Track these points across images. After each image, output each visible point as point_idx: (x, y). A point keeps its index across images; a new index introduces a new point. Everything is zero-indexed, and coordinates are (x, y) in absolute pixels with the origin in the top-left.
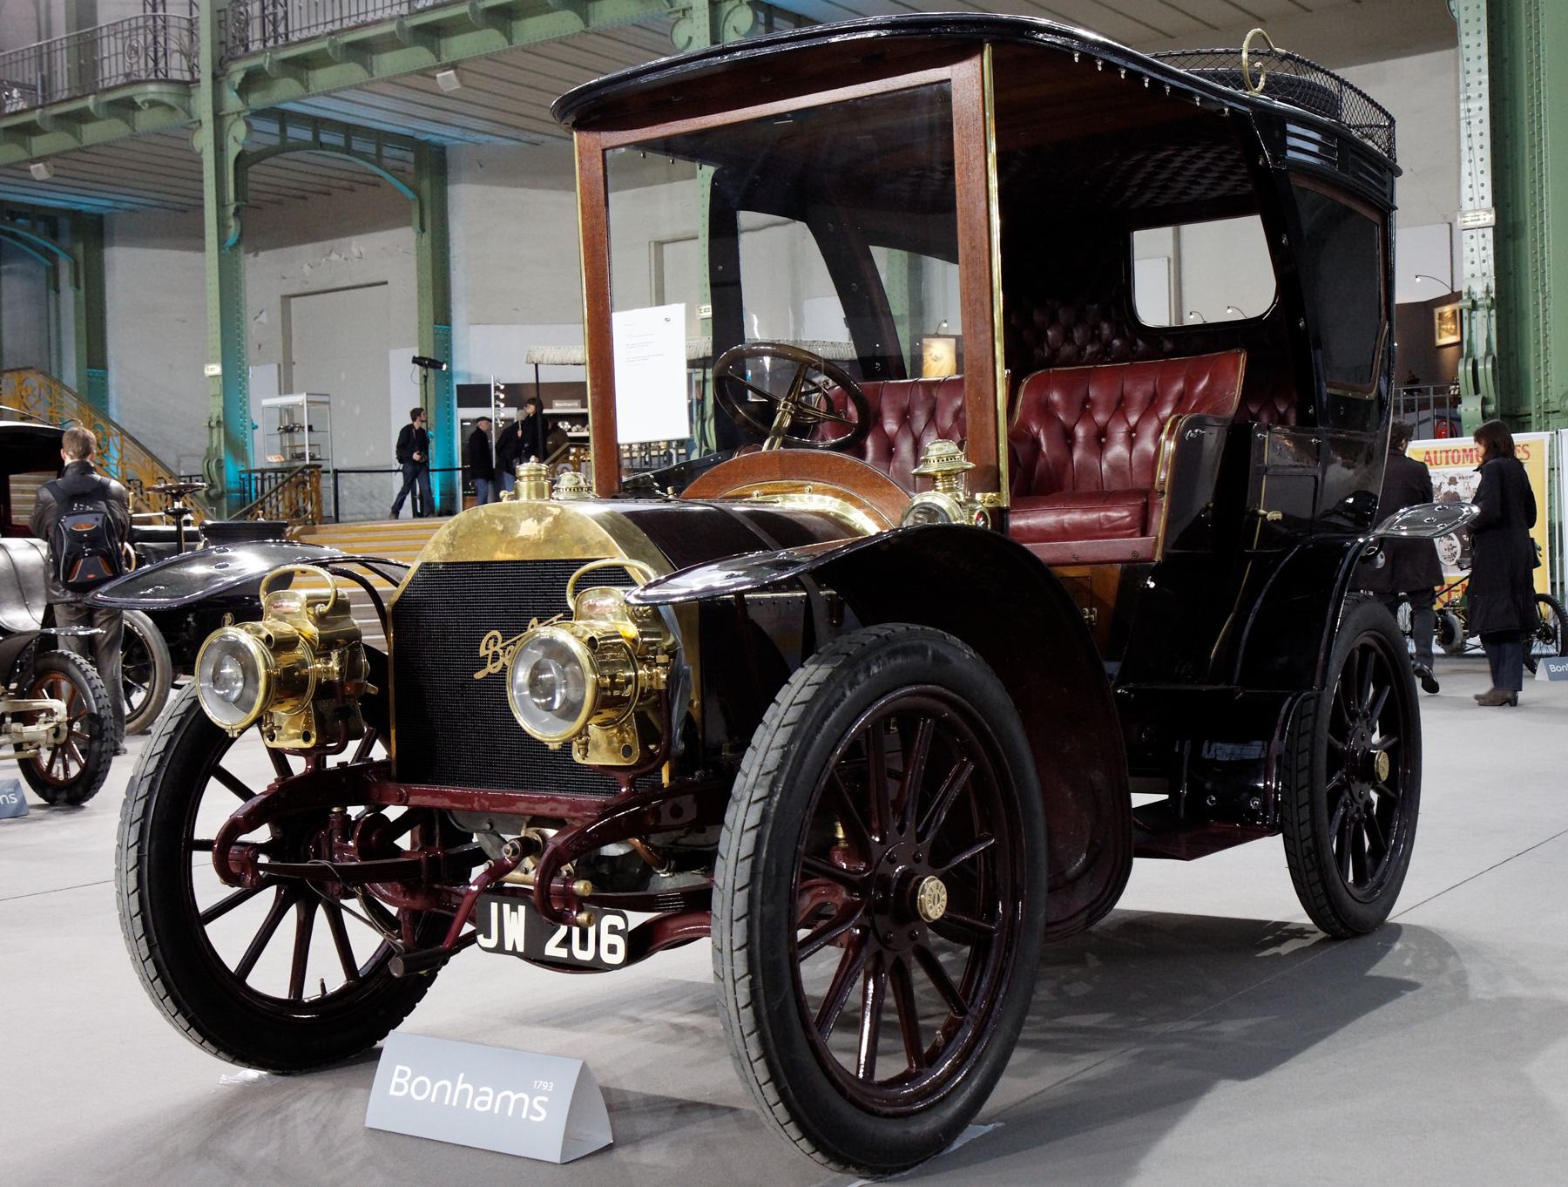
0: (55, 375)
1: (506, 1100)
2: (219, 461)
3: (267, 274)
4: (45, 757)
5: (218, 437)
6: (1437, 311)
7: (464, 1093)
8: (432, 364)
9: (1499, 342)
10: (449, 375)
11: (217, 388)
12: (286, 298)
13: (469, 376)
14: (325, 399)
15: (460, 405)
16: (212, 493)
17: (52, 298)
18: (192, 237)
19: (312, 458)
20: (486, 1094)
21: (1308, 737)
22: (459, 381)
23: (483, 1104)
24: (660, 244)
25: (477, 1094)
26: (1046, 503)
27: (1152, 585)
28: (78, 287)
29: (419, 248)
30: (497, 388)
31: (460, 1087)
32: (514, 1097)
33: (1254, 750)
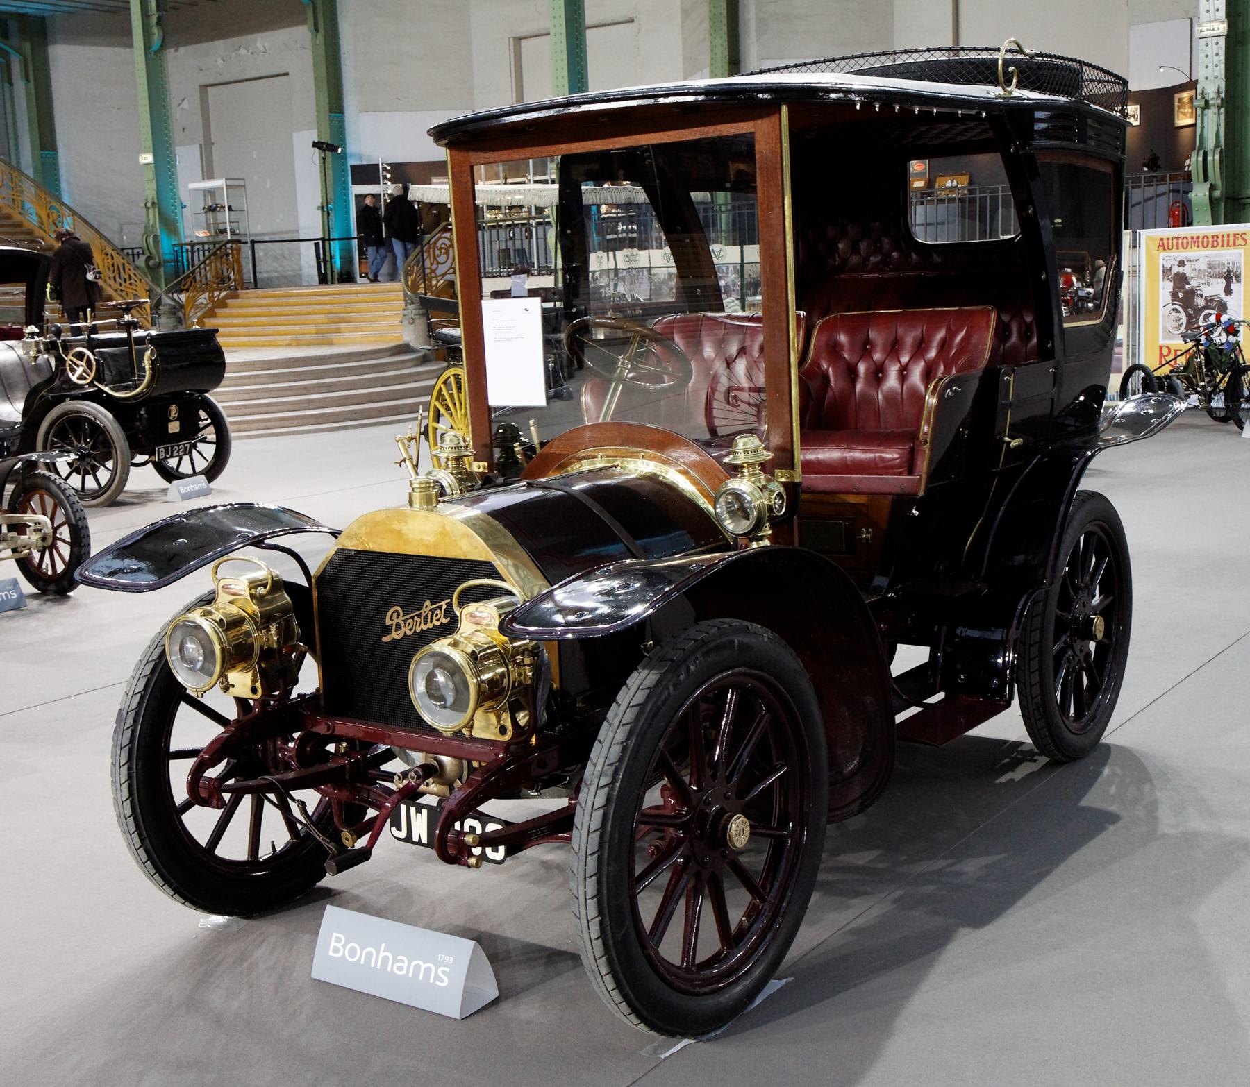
0: (14, 163)
1: (417, 967)
2: (156, 237)
3: (188, 65)
5: (153, 216)
6: (1177, 96)
7: (385, 959)
8: (329, 147)
9: (1226, 134)
10: (344, 156)
11: (150, 174)
12: (204, 87)
13: (360, 157)
14: (241, 183)
15: (354, 183)
16: (151, 263)
17: (7, 90)
18: (122, 35)
19: (233, 233)
20: (402, 961)
21: (1039, 618)
22: (352, 161)
23: (400, 969)
24: (518, 40)
25: (395, 961)
26: (833, 442)
27: (916, 513)
28: (28, 80)
29: (314, 46)
30: (384, 169)
31: (382, 954)
32: (423, 966)
33: (997, 635)
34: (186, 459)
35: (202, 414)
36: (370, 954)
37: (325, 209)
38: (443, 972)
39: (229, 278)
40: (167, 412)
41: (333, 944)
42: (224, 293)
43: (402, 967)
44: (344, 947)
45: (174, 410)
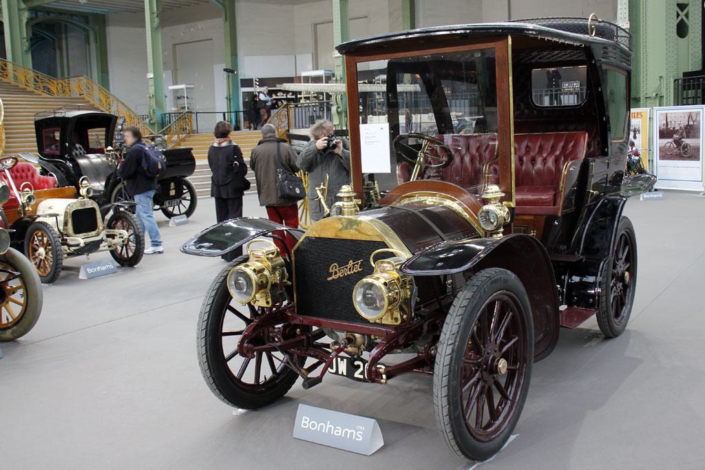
1: (347, 432)
4: (120, 249)
5: (153, 102)
10: (237, 75)
11: (151, 82)
12: (175, 45)
15: (242, 86)
16: (151, 122)
17: (87, 47)
19: (188, 108)
22: (240, 77)
23: (338, 433)
28: (97, 42)
30: (256, 80)
31: (328, 426)
34: (177, 207)
35: (185, 187)
36: (322, 427)
37: (229, 99)
38: (360, 434)
39: (186, 129)
40: (169, 186)
41: (303, 422)
42: (184, 136)
43: (339, 432)
44: (309, 423)
45: (172, 185)
